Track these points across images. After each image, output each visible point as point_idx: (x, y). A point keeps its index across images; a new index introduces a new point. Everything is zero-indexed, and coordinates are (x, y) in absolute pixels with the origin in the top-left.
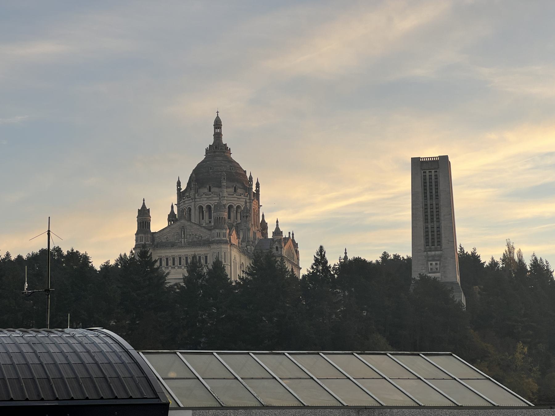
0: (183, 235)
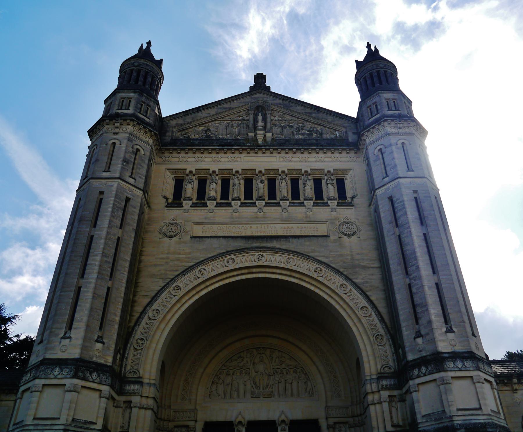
0: (260, 123)
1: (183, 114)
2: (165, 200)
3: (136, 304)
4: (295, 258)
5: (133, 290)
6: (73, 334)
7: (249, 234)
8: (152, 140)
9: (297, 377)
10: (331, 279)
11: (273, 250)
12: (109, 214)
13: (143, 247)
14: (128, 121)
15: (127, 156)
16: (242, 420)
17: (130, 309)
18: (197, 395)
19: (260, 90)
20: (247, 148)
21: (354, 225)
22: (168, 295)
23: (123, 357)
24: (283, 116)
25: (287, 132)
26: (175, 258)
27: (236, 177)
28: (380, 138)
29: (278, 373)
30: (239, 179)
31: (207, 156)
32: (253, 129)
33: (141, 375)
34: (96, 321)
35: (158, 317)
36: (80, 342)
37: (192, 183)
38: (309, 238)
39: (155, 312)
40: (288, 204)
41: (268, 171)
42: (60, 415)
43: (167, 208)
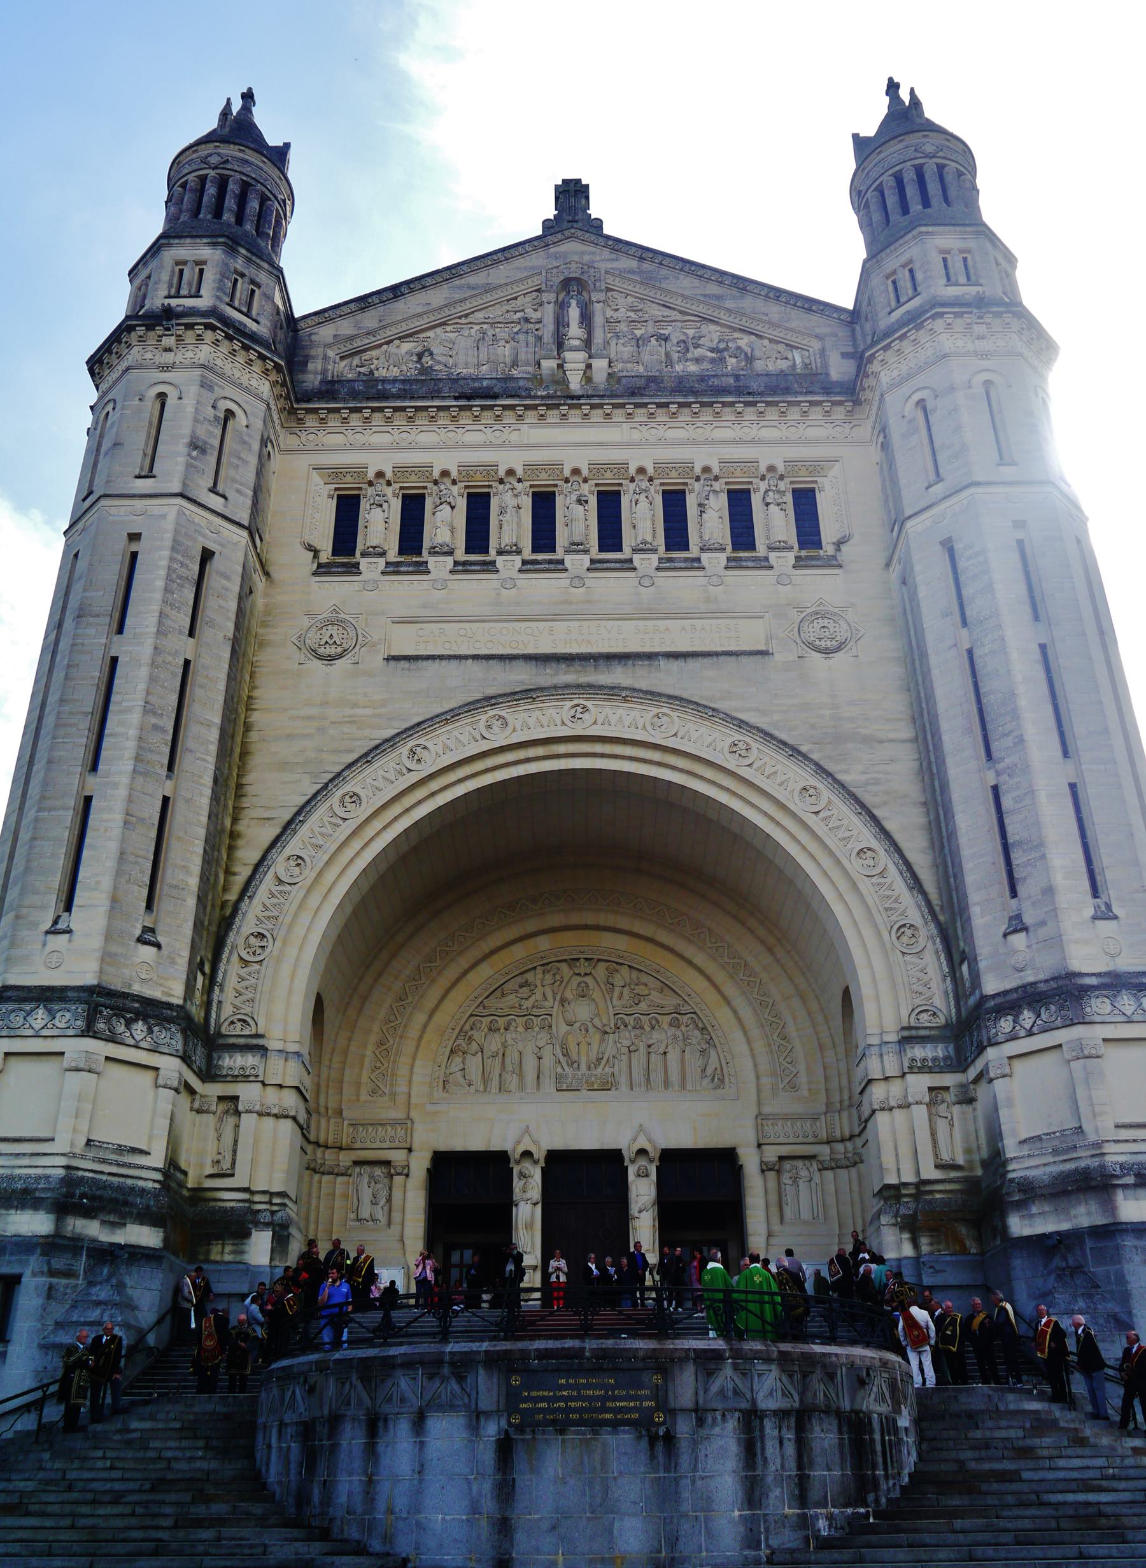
1: (352, 306)
2: (312, 554)
3: (240, 842)
4: (674, 714)
5: (230, 804)
6: (76, 919)
7: (546, 647)
8: (267, 384)
9: (681, 1037)
10: (776, 773)
11: (612, 692)
12: (158, 596)
13: (253, 688)
14: (199, 329)
15: (201, 432)
16: (533, 1149)
17: (225, 857)
18: (410, 1081)
19: (573, 231)
20: (537, 402)
21: (842, 623)
22: (326, 819)
23: (212, 980)
24: (641, 306)
25: (653, 353)
26: (344, 717)
27: (508, 486)
28: (920, 370)
29: (630, 1027)
30: (516, 492)
31: (424, 428)
32: (555, 348)
33: (260, 1031)
34: (137, 888)
35: (303, 877)
36: (97, 943)
37: (385, 505)
38: (715, 659)
39: (293, 863)
40: (655, 563)
41: (598, 468)
42: (55, 1131)
43: (317, 579)
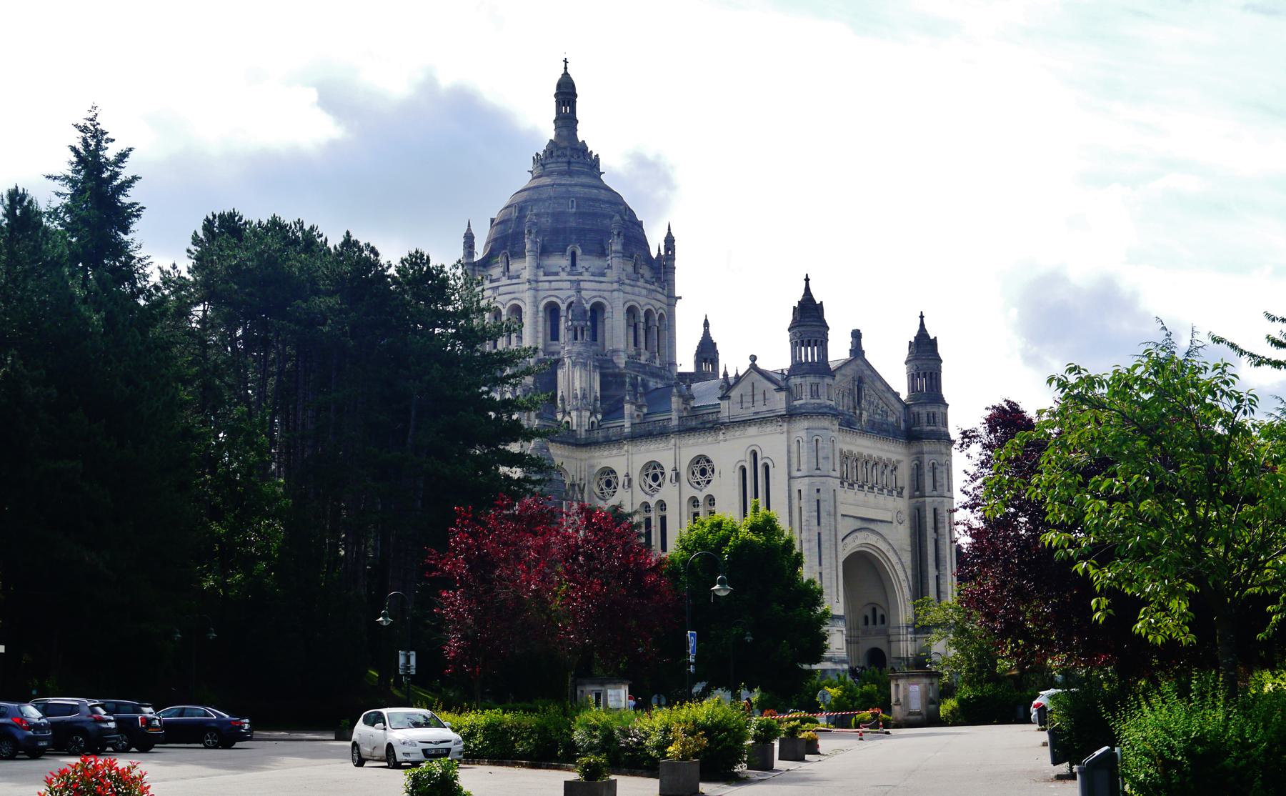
11: (873, 531)
